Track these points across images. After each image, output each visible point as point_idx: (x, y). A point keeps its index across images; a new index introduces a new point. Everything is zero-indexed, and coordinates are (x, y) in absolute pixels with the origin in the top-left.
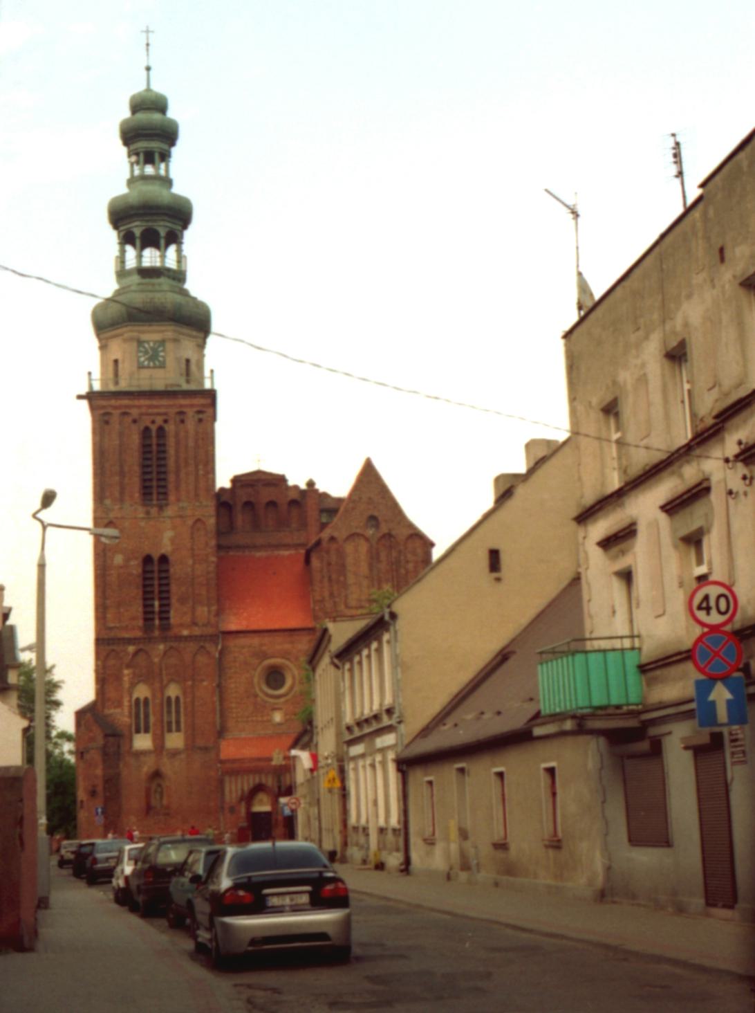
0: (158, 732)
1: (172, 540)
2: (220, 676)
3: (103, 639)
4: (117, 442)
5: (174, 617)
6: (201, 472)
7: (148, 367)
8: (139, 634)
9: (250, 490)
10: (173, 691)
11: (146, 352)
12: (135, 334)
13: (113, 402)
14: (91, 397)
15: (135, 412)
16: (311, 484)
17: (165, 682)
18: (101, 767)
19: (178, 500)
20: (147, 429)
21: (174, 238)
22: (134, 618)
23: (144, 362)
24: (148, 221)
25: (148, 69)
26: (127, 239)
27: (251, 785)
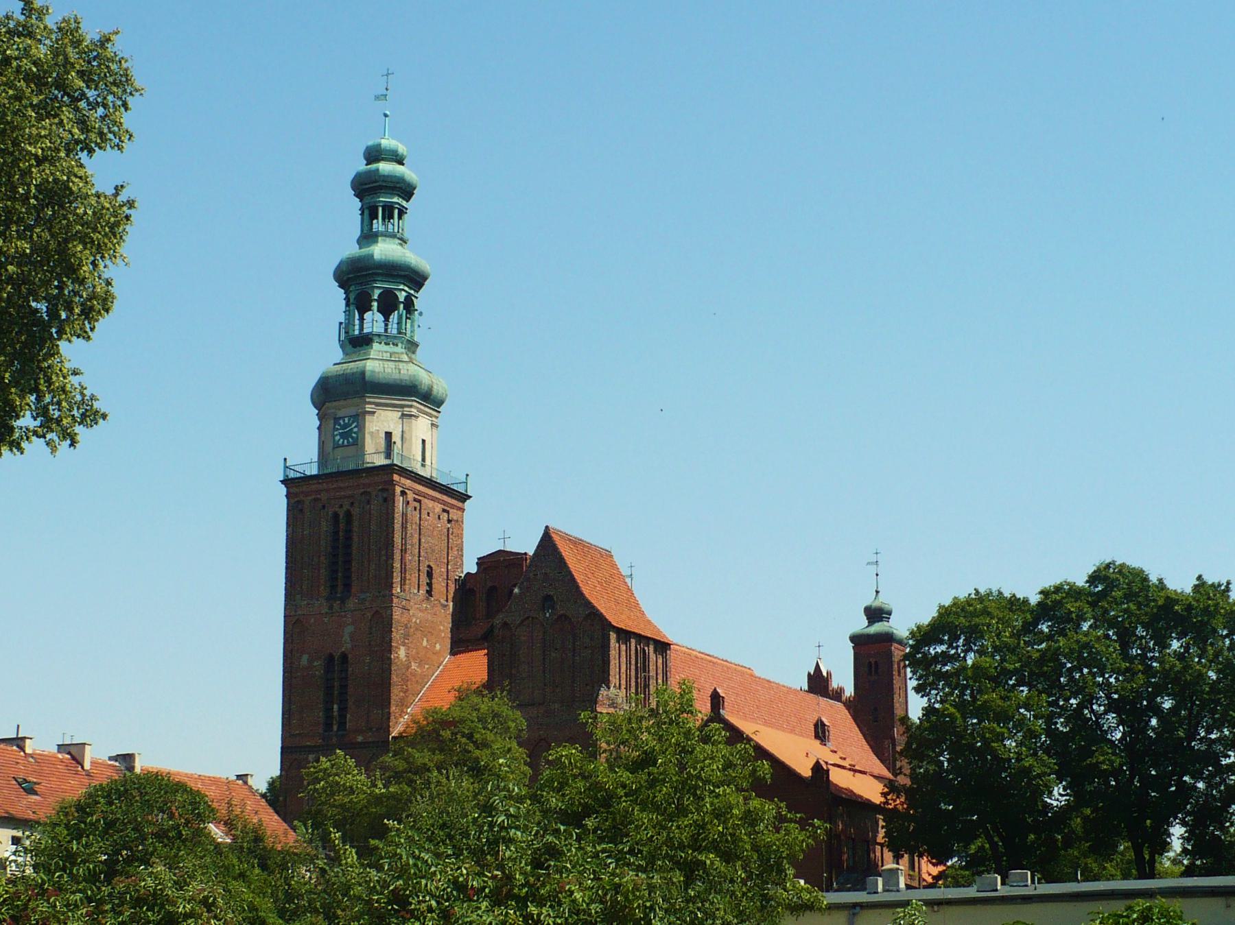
7: (343, 446)
20: (336, 515)
24: (361, 284)
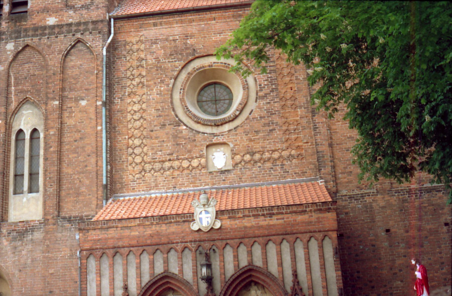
2: (110, 87)
17: (13, 106)
27: (146, 279)
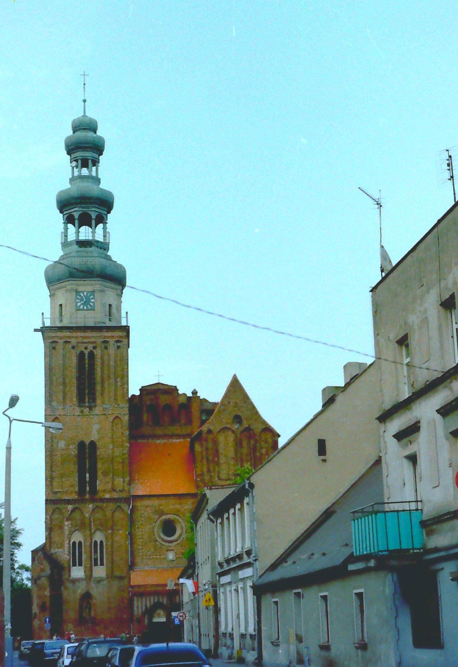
0: (88, 566)
1: (99, 431)
2: (131, 527)
3: (51, 500)
4: (62, 362)
5: (100, 486)
6: (119, 384)
8: (76, 497)
9: (152, 397)
10: (99, 537)
11: (82, 300)
12: (75, 287)
13: (59, 334)
14: (43, 330)
15: (73, 341)
16: (195, 392)
17: (93, 531)
18: (48, 589)
19: (103, 403)
21: (101, 219)
22: (72, 486)
23: (80, 306)
25: (85, 101)
26: (70, 220)
